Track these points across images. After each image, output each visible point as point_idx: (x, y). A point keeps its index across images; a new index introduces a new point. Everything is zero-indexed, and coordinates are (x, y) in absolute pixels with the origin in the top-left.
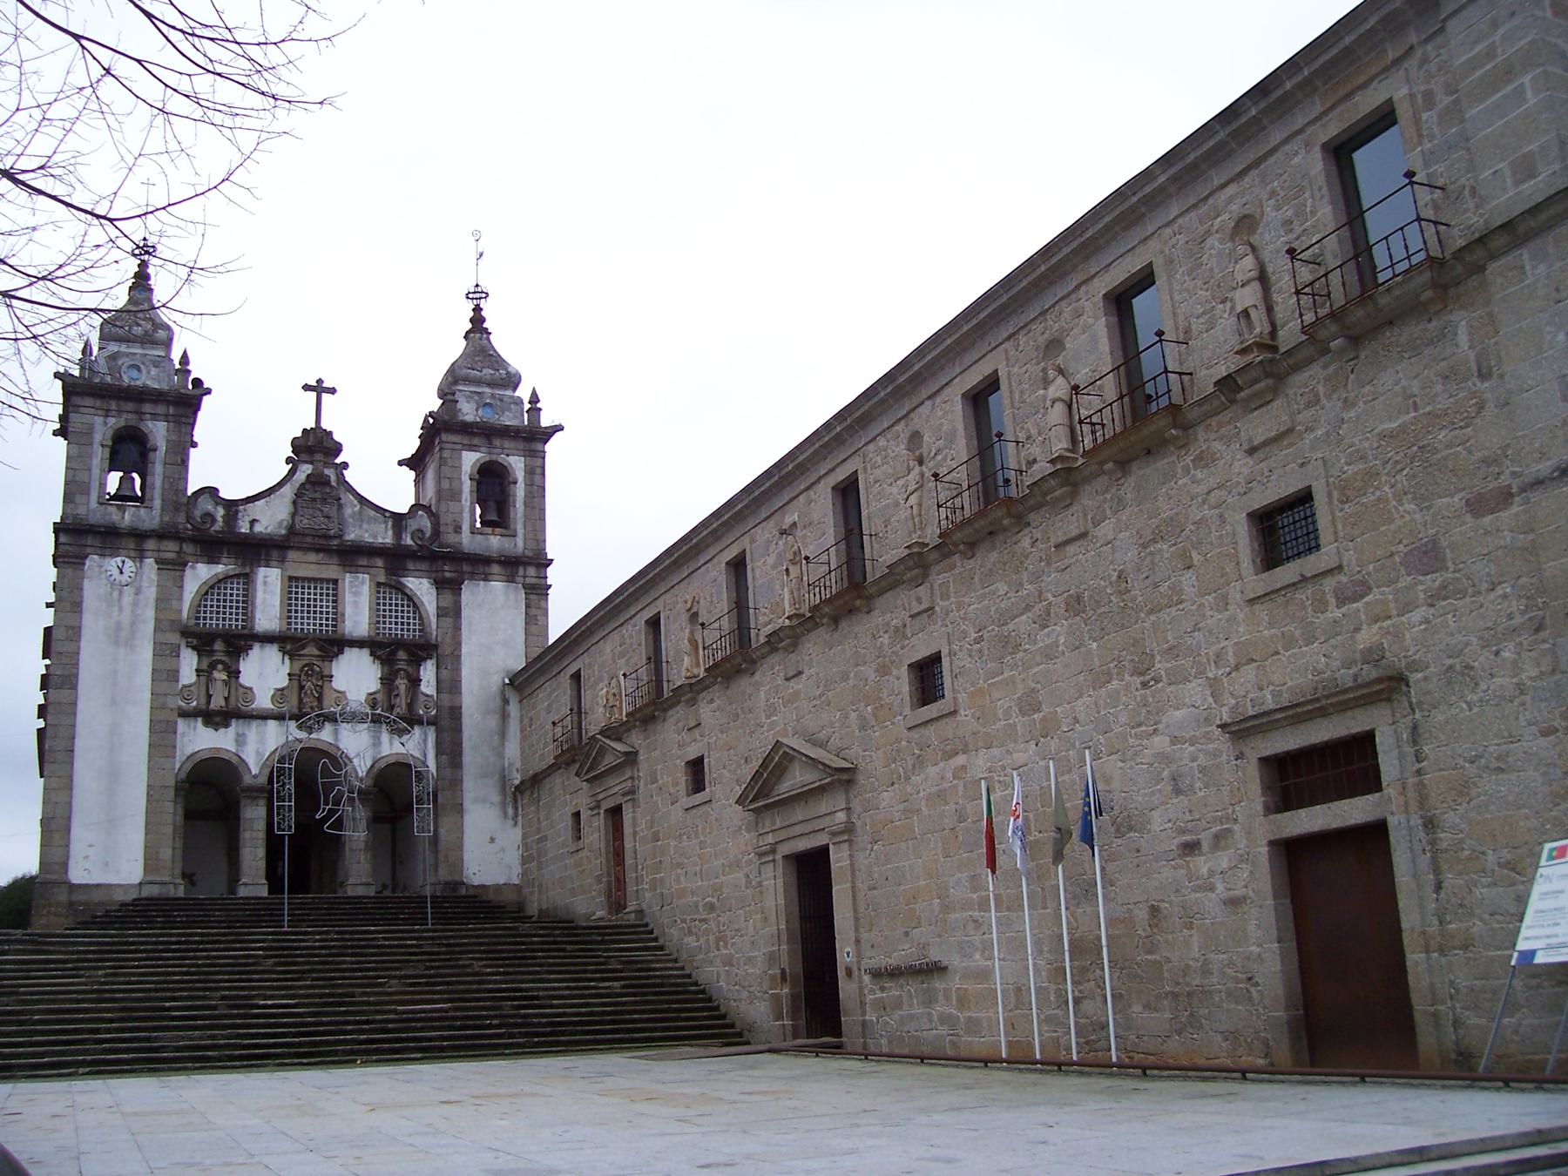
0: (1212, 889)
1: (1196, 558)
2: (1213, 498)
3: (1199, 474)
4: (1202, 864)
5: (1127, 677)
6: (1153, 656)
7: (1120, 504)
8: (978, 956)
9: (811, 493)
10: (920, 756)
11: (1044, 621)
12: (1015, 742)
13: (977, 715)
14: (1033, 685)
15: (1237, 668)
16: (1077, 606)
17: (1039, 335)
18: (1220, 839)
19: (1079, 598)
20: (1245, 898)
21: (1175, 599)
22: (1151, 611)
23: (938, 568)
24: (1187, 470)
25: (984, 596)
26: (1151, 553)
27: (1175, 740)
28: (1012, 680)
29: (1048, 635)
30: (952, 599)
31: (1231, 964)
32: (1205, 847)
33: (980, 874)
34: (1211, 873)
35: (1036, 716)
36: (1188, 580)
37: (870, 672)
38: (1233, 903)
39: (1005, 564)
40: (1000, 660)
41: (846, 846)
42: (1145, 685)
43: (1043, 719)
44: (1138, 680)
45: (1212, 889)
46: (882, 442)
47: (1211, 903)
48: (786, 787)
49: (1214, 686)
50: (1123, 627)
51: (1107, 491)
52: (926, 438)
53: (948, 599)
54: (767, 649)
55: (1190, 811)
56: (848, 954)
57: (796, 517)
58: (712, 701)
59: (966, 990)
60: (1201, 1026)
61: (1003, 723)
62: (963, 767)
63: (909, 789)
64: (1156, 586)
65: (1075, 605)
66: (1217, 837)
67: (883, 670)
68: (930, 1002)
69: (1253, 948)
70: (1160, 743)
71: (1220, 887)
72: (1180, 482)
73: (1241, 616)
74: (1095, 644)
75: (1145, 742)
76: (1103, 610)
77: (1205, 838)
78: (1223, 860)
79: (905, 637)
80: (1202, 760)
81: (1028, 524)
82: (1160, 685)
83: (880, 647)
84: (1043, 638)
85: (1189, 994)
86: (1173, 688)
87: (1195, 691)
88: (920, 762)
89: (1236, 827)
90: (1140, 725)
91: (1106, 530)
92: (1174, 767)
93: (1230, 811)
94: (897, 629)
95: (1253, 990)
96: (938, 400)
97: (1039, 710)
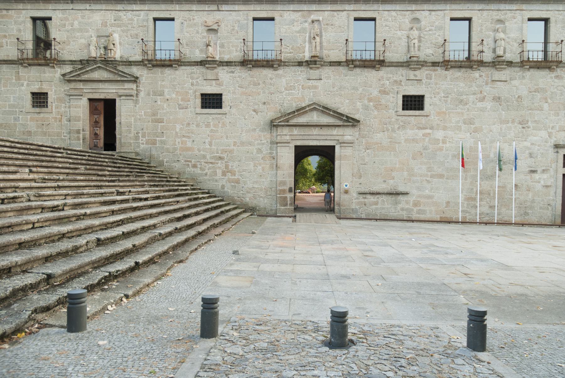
0: (539, 182)
1: (549, 101)
2: (559, 88)
3: (556, 80)
4: (536, 176)
5: (516, 124)
6: (528, 121)
7: (523, 77)
8: (427, 191)
9: (335, 13)
10: (403, 125)
11: (483, 99)
12: (460, 131)
13: (442, 119)
14: (472, 117)
15: (558, 131)
16: (498, 100)
17: (496, 15)
18: (544, 171)
19: (499, 98)
20: (551, 186)
21: (540, 109)
22: (530, 110)
23: (426, 68)
24: (552, 78)
25: (451, 85)
26: (533, 95)
27: (532, 144)
28: (462, 113)
29: (482, 104)
30: (433, 80)
31: (543, 200)
32: (539, 172)
33: (433, 167)
34: (540, 178)
35: (472, 126)
36: (546, 106)
37: (375, 93)
38: (547, 187)
39: (465, 78)
40: (457, 106)
41: (351, 148)
42: (523, 128)
43: (476, 127)
44: (521, 126)
45: (539, 182)
46: (394, 13)
47: (538, 187)
48: (302, 120)
49: (550, 134)
50: (517, 110)
51: (518, 72)
52: (423, 23)
53: (431, 79)
54: (297, 64)
55: (535, 163)
56: (346, 186)
57: (321, 19)
58: (233, 72)
59: (419, 201)
60: (529, 215)
61: (454, 124)
62: (429, 134)
63: (395, 135)
64: (533, 103)
65: (497, 99)
66: (544, 170)
67: (384, 92)
68: (396, 204)
69: (551, 198)
70: (527, 144)
71: (542, 182)
72: (548, 80)
73: (563, 119)
74: (504, 112)
75: (520, 142)
76: (509, 104)
77: (539, 170)
78: (545, 176)
79: (400, 84)
80: (542, 151)
81: (480, 70)
82: (529, 129)
83: (383, 85)
84: (479, 105)
85: (525, 207)
86: (535, 131)
87: (544, 134)
88: (403, 127)
89: (551, 169)
90: (519, 138)
91: (515, 82)
92: (531, 151)
93: (550, 164)
94: (396, 81)
95: (549, 207)
96: (433, 13)
97: (473, 125)
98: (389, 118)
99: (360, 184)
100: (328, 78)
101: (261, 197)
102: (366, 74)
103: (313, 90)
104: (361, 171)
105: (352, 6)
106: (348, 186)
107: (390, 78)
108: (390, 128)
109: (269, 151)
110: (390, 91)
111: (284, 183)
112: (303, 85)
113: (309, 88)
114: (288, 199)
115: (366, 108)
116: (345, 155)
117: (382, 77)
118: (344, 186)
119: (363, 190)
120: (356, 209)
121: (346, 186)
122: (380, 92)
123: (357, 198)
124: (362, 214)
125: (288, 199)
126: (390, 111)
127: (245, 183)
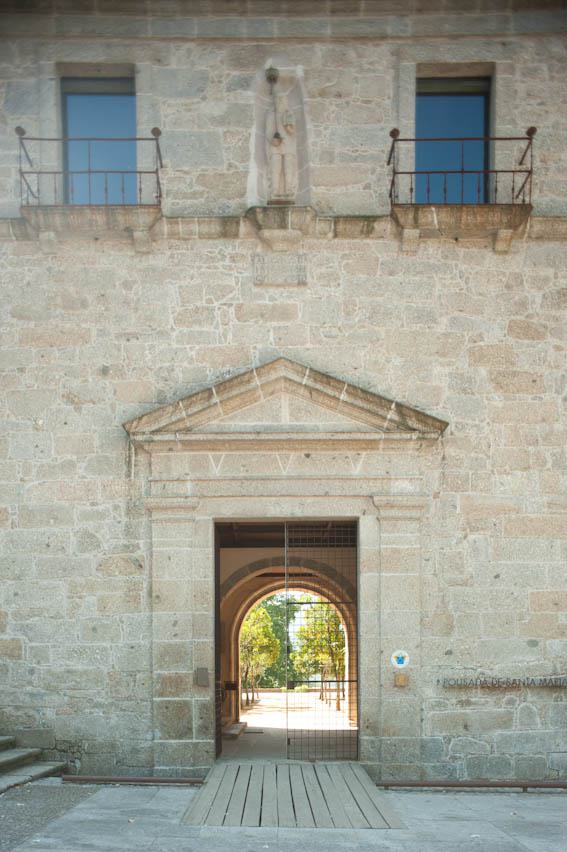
41: (414, 525)
56: (400, 660)
98: (544, 420)
99: (449, 653)
100: (330, 278)
101: (98, 705)
102: (463, 267)
103: (275, 324)
104: (451, 607)
105: (409, 20)
106: (407, 660)
107: (546, 280)
108: (548, 455)
109: (123, 541)
110: (545, 327)
111: (175, 654)
112: (239, 307)
113: (262, 316)
114: (195, 712)
115: (464, 385)
116: (396, 551)
117: (518, 279)
118: (394, 661)
119: (458, 672)
120: (434, 741)
121: (400, 660)
122: (510, 328)
123: (439, 704)
124: (454, 758)
125: (195, 712)
126: (547, 397)
127: (40, 655)
